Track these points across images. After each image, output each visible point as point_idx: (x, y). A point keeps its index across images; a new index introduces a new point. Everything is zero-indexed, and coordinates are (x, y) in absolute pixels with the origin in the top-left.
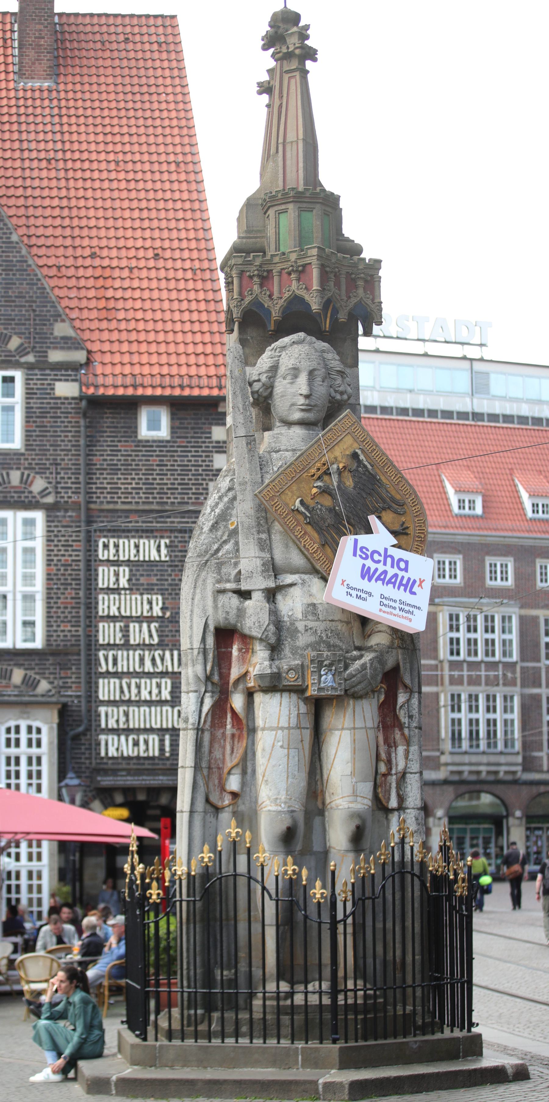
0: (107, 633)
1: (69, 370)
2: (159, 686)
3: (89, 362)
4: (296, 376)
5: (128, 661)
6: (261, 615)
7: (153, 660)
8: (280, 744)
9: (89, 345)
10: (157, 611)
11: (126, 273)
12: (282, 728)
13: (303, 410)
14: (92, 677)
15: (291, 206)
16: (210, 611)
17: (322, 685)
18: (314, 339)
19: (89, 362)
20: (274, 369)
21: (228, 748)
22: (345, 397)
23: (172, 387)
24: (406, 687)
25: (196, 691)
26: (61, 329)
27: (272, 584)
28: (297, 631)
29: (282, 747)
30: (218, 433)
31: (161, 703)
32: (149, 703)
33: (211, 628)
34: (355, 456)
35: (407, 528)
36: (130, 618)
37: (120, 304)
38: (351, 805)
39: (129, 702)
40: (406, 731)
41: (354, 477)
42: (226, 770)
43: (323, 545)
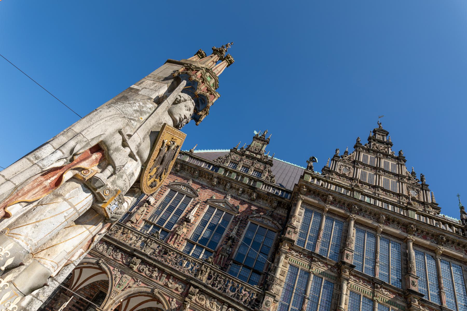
6: (125, 159)
8: (66, 215)
12: (75, 209)
13: (180, 119)
15: (214, 79)
16: (107, 133)
17: (111, 208)
20: (185, 100)
21: (37, 190)
25: (63, 153)
27: (135, 153)
28: (122, 177)
29: (65, 217)
33: (101, 139)
38: (51, 269)
42: (20, 199)
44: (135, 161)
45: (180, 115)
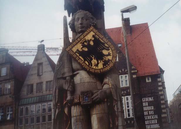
0: (146, 113)
1: (134, 73)
2: (155, 121)
3: (138, 72)
4: (79, 20)
5: (149, 117)
7: (153, 117)
9: (138, 69)
10: (153, 109)
11: (142, 58)
13: (81, 28)
14: (144, 120)
18: (84, 11)
19: (138, 72)
22: (94, 24)
23: (150, 73)
24: (115, 100)
26: (133, 67)
27: (71, 74)
30: (159, 80)
31: (156, 124)
32: (154, 124)
34: (93, 36)
35: (110, 54)
36: (149, 110)
37: (142, 63)
39: (150, 124)
40: (117, 113)
41: (93, 42)
43: (85, 61)
44: (77, 75)
45: (78, 27)
